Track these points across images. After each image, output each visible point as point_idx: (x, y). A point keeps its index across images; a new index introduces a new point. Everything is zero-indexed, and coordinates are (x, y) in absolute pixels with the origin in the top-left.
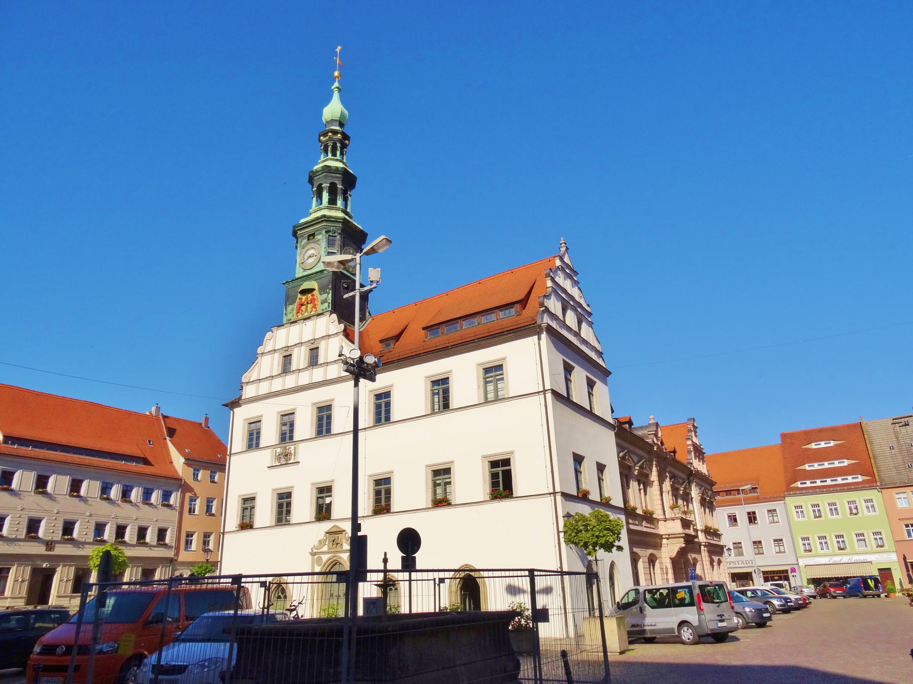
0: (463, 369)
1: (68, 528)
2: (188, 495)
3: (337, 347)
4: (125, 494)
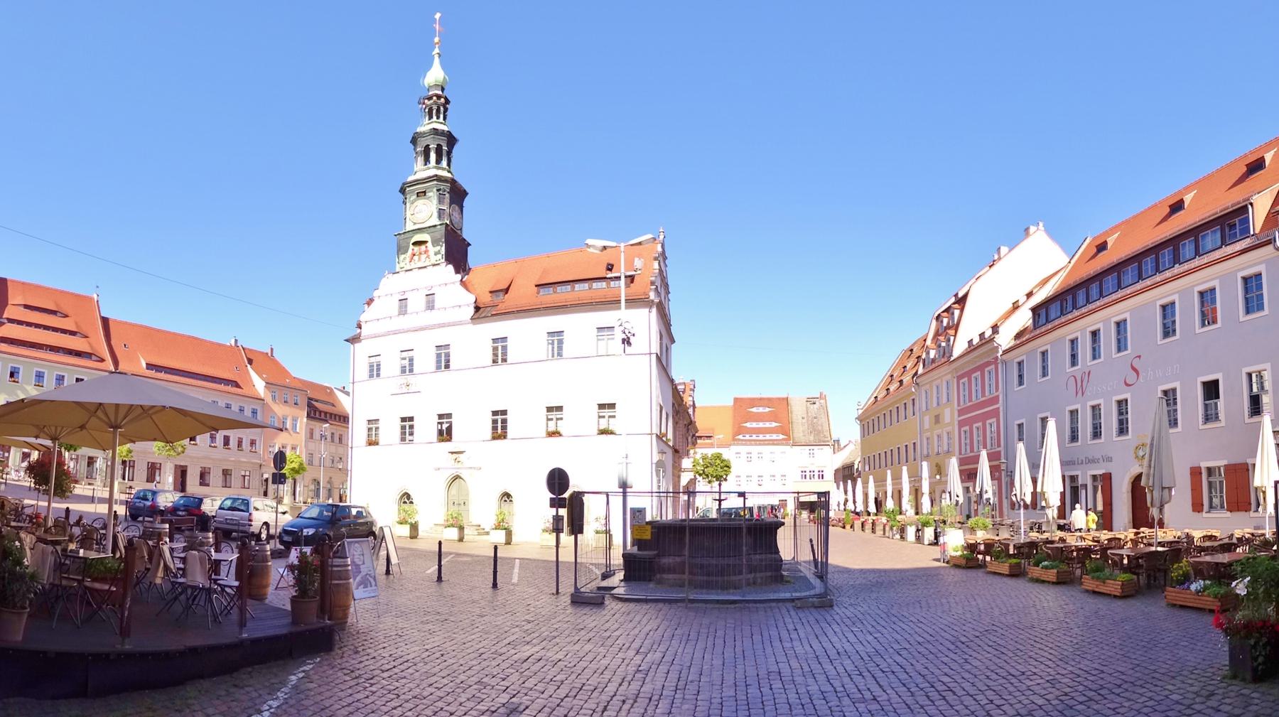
0: (579, 326)
3: (454, 296)
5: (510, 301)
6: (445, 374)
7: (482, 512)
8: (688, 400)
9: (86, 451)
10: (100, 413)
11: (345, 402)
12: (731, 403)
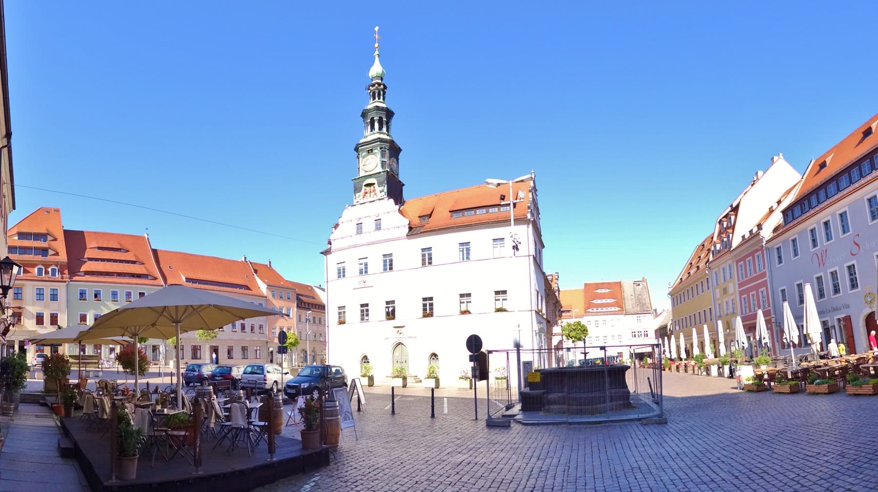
5: (433, 222)
6: (389, 274)
7: (418, 367)
8: (554, 286)
9: (151, 342)
10: (165, 313)
11: (322, 296)
12: (583, 287)
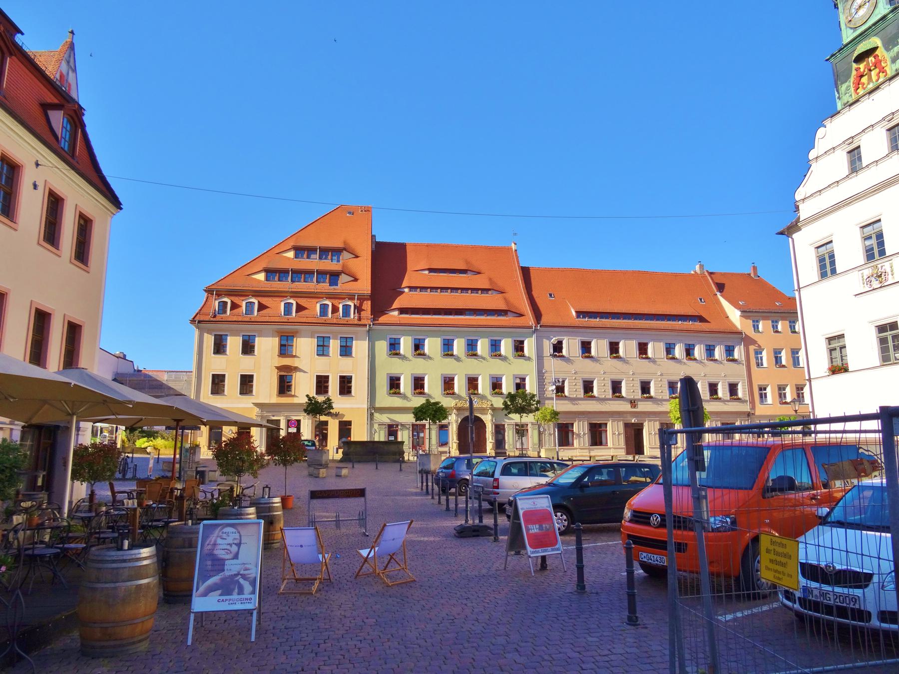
1: (645, 388)
2: (752, 348)
4: (689, 352)
